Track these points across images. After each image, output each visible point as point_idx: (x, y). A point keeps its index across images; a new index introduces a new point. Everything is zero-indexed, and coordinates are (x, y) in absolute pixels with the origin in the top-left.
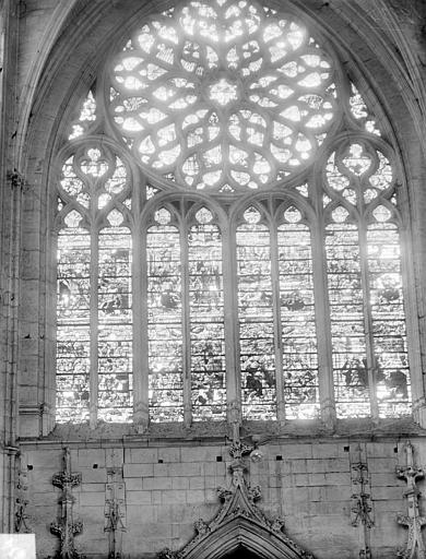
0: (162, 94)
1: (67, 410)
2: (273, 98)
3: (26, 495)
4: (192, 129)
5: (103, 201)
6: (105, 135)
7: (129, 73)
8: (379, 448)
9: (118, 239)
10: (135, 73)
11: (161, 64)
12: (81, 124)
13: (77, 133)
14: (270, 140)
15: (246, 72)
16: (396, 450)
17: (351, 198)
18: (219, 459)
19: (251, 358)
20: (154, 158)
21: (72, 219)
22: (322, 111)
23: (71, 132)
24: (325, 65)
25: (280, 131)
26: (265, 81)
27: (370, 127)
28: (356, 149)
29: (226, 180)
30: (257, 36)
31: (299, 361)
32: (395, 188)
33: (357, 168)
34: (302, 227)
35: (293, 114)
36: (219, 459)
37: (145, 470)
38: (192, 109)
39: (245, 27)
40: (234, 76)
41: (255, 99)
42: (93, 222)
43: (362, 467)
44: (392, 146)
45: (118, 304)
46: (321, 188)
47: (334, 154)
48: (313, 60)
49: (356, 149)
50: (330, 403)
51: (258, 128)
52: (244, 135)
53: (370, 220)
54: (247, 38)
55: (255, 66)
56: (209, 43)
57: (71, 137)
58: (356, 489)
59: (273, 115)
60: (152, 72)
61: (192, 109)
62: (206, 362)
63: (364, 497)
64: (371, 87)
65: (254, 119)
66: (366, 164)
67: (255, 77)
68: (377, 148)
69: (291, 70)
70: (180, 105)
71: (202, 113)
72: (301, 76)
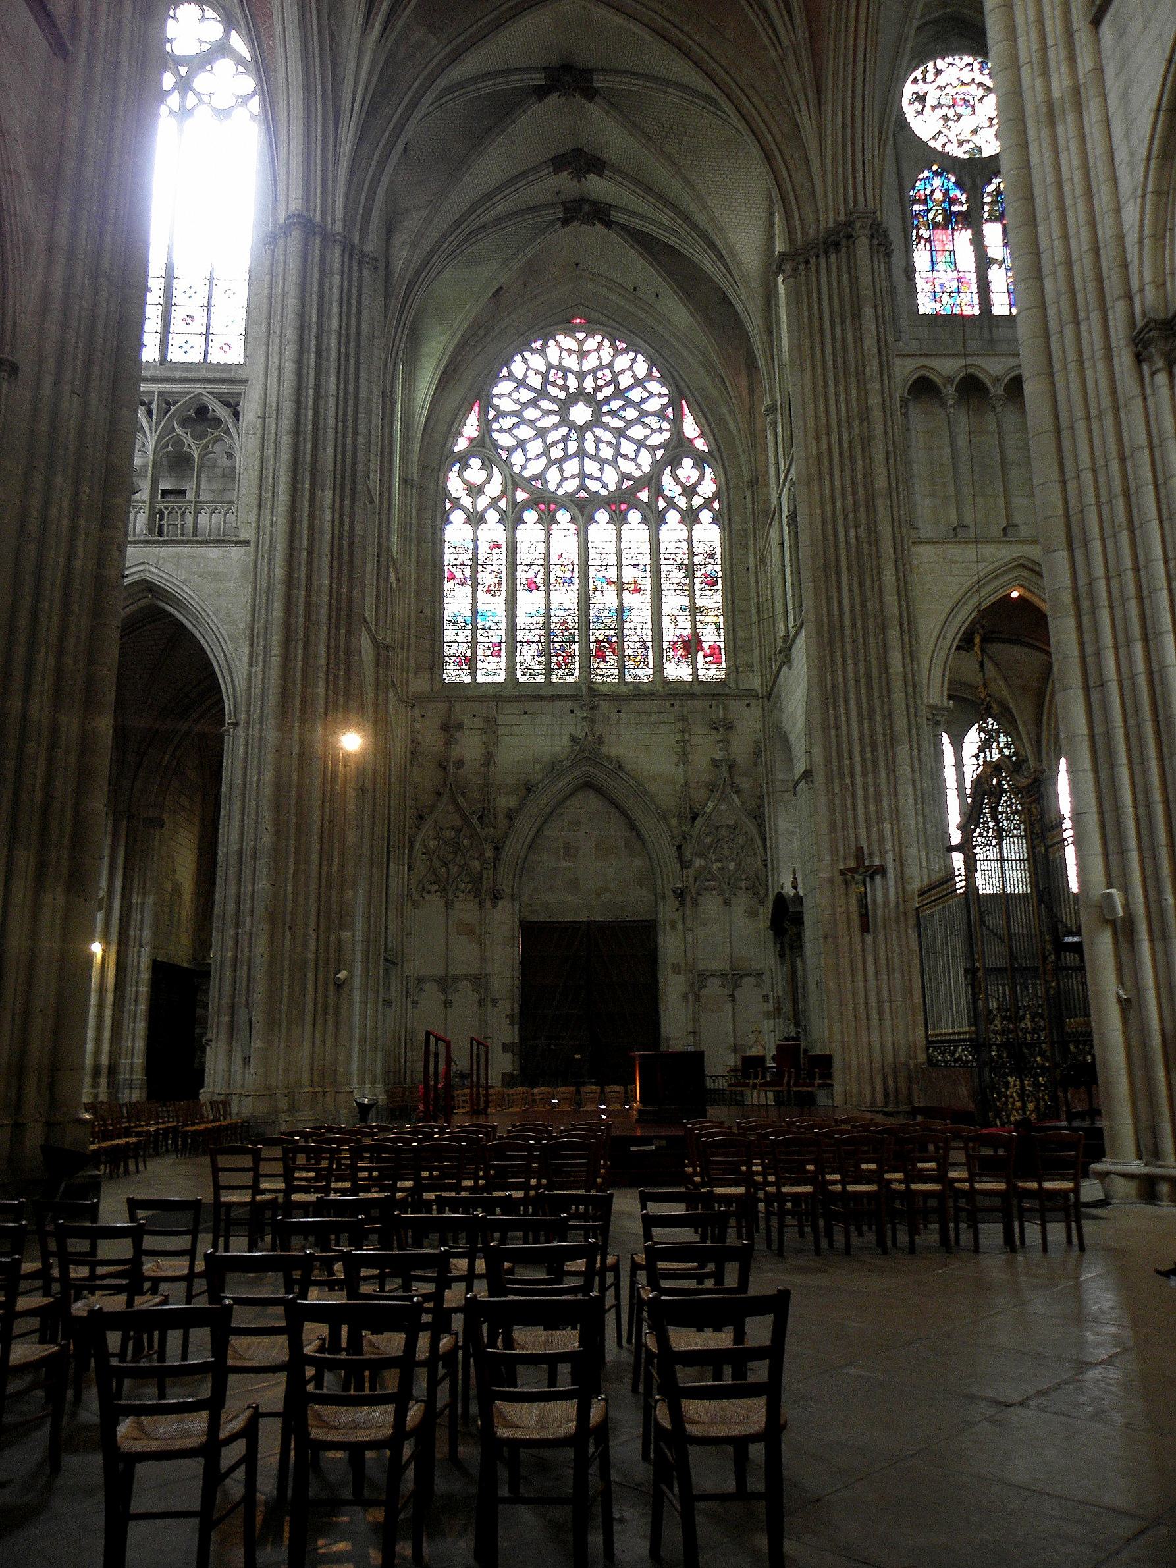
0: (531, 414)
1: (454, 674)
2: (623, 419)
3: (420, 737)
4: (555, 444)
5: (483, 502)
6: (484, 447)
7: (504, 394)
8: (698, 704)
9: (493, 530)
11: (531, 389)
13: (461, 445)
14: (618, 453)
15: (600, 396)
17: (682, 502)
18: (572, 712)
21: (458, 517)
22: (661, 430)
24: (665, 391)
26: (615, 405)
27: (700, 444)
28: (687, 462)
29: (582, 486)
30: (610, 366)
32: (717, 496)
35: (637, 432)
36: (572, 712)
38: (556, 427)
39: (599, 357)
40: (590, 400)
41: (606, 419)
43: (684, 719)
46: (658, 491)
48: (654, 387)
49: (687, 462)
50: (659, 668)
51: (609, 444)
52: (597, 449)
53: (697, 520)
54: (601, 367)
57: (456, 449)
58: (678, 737)
60: (525, 395)
61: (556, 427)
63: (684, 741)
66: (695, 474)
68: (704, 461)
69: (636, 394)
71: (564, 431)
72: (643, 400)
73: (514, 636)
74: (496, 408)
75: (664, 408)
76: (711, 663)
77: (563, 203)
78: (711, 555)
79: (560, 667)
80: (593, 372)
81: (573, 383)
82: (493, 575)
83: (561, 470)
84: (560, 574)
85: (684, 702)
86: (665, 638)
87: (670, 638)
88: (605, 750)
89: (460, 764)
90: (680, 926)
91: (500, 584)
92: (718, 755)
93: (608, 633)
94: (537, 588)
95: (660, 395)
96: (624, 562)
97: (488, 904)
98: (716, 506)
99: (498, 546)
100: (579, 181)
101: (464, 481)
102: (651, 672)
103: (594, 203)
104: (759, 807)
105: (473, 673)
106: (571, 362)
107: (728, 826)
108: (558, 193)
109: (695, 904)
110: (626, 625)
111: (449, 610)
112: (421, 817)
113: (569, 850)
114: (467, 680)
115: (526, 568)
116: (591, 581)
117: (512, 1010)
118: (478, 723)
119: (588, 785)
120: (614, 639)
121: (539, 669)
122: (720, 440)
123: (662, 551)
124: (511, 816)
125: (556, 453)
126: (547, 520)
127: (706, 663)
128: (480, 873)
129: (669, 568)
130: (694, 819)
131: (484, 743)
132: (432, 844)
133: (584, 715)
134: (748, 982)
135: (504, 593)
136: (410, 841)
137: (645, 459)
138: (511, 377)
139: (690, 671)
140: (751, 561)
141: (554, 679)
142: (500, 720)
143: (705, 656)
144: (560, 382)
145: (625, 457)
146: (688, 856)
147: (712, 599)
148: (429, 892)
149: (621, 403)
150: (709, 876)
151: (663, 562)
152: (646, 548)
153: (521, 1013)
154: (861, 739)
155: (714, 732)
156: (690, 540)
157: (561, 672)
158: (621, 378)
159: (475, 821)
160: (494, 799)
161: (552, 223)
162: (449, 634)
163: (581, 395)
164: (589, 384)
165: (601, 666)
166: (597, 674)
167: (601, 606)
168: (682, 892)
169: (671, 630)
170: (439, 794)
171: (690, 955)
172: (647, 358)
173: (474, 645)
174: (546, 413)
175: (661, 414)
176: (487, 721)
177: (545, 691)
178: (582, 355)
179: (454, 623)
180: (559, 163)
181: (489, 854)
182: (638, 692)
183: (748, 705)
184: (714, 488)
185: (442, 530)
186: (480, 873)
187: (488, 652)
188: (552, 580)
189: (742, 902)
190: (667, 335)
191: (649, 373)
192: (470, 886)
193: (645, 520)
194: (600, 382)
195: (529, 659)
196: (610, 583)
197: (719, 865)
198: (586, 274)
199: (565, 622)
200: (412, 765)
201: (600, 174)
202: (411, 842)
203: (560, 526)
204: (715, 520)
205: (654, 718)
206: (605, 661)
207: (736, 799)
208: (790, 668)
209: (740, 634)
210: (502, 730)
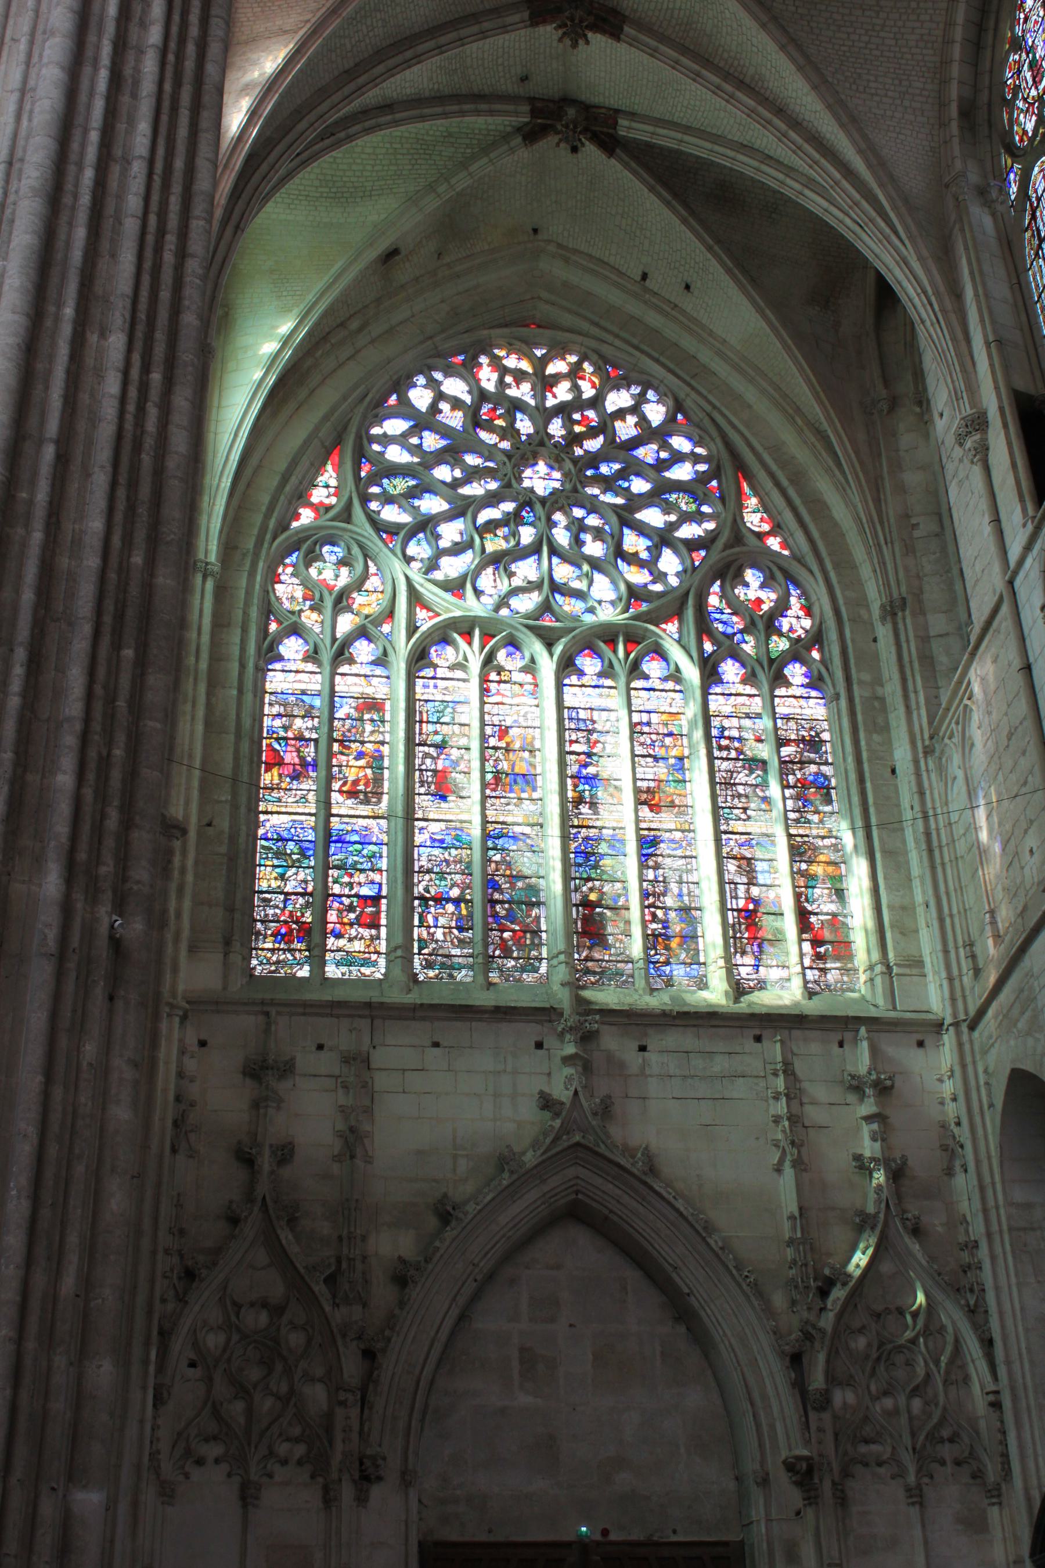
0: (443, 473)
4: (491, 526)
5: (345, 624)
10: (401, 440)
11: (444, 431)
12: (315, 507)
13: (306, 516)
17: (749, 647)
19: (590, 884)
21: (292, 648)
22: (698, 517)
23: (297, 516)
25: (633, 542)
30: (596, 402)
32: (817, 638)
33: (759, 601)
35: (653, 517)
39: (576, 388)
42: (326, 656)
44: (811, 572)
45: (366, 785)
47: (718, 583)
48: (681, 443)
49: (752, 576)
51: (598, 534)
52: (578, 543)
53: (779, 679)
54: (578, 404)
55: (594, 445)
56: (517, 406)
59: (625, 517)
60: (431, 441)
61: (492, 499)
62: (513, 886)
64: (777, 484)
65: (593, 521)
66: (769, 598)
67: (594, 460)
70: (474, 489)
71: (509, 507)
72: (661, 466)
73: (409, 885)
75: (701, 479)
77: (531, 100)
78: (813, 744)
79: (507, 954)
80: (563, 410)
81: (525, 426)
82: (362, 763)
87: (741, 903)
89: (285, 1153)
95: (696, 459)
97: (347, 1492)
98: (815, 655)
101: (306, 583)
103: (587, 109)
105: (318, 961)
106: (523, 392)
108: (524, 79)
109: (842, 1500)
111: (272, 823)
112: (190, 1275)
114: (304, 972)
115: (432, 751)
116: (569, 781)
118: (327, 1063)
122: (816, 534)
123: (715, 732)
125: (495, 544)
128: (330, 1415)
130: (824, 1293)
131: (342, 1109)
132: (213, 1341)
133: (570, 1049)
136: (161, 1333)
137: (670, 563)
138: (406, 410)
142: (379, 1058)
144: (500, 422)
145: (632, 559)
146: (817, 1380)
148: (200, 1462)
149: (617, 466)
151: (716, 753)
155: (851, 1098)
158: (618, 424)
159: (320, 1288)
160: (364, 1238)
161: (506, 137)
162: (266, 878)
163: (542, 444)
166: (588, 971)
168: (810, 1471)
169: (741, 890)
170: (234, 1221)
173: (321, 898)
174: (473, 475)
177: (484, 999)
178: (545, 383)
179: (278, 855)
181: (352, 1367)
184: (807, 623)
185: (262, 672)
186: (330, 1415)
187: (352, 916)
190: (705, 356)
192: (300, 1450)
194: (578, 429)
195: (439, 934)
197: (888, 1403)
198: (552, 248)
200: (174, 1150)
201: (616, 34)
202: (165, 1335)
204: (815, 682)
207: (915, 1247)
210: (381, 1081)
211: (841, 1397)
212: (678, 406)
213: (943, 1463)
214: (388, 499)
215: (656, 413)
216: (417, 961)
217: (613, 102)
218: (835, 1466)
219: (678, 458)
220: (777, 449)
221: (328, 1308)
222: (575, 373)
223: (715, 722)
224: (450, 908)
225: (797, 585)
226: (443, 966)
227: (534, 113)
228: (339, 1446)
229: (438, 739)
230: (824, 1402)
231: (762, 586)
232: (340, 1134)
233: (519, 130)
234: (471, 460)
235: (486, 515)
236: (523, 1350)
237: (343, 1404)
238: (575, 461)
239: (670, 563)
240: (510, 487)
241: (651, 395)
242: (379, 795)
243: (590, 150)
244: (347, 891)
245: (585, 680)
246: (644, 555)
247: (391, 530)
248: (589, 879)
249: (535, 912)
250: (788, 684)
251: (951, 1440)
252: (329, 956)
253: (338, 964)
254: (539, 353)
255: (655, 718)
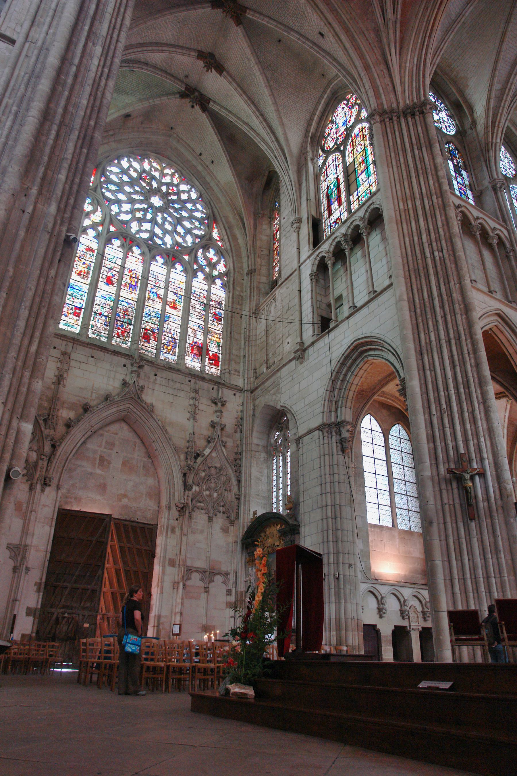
4: (139, 210)
8: (206, 385)
10: (117, 174)
11: (130, 177)
16: (213, 389)
20: (118, 214)
22: (200, 229)
25: (179, 229)
29: (151, 238)
30: (177, 186)
31: (170, 333)
32: (227, 274)
33: (212, 259)
34: (182, 274)
35: (187, 224)
36: (125, 366)
37: (83, 359)
40: (164, 196)
43: (196, 392)
48: (199, 206)
50: (181, 357)
51: (170, 223)
52: (163, 224)
53: (214, 282)
55: (174, 198)
56: (153, 178)
58: (192, 402)
59: (179, 221)
61: (141, 202)
62: (124, 317)
64: (224, 227)
65: (169, 219)
66: (215, 259)
67: (173, 202)
69: (189, 206)
71: (146, 206)
73: (92, 308)
74: (107, 177)
75: (203, 219)
76: (212, 364)
77: (187, 85)
78: (220, 303)
79: (119, 336)
80: (167, 184)
82: (85, 266)
83: (141, 225)
84: (129, 281)
85: (198, 382)
86: (188, 341)
87: (191, 342)
88: (144, 397)
90: (178, 531)
91: (88, 273)
92: (216, 419)
93: (153, 326)
94: (112, 283)
95: (203, 213)
96: (170, 289)
97: (39, 487)
99: (93, 251)
100: (207, 71)
102: (176, 358)
103: (201, 95)
104: (236, 460)
106: (157, 174)
107: (216, 467)
109: (190, 517)
110: (166, 326)
113: (103, 462)
115: (107, 270)
116: (147, 292)
117: (41, 579)
118: (56, 353)
119: (124, 420)
120: (156, 331)
121: (104, 333)
122: (232, 245)
124: (69, 425)
125: (139, 215)
126: (127, 248)
127: (209, 363)
129: (195, 302)
130: (196, 458)
131: (58, 369)
134: (219, 579)
135: (89, 279)
137: (189, 239)
138: (119, 166)
139: (199, 365)
140: (246, 312)
141: (113, 342)
142: (73, 356)
143: (210, 359)
145: (179, 234)
146: (190, 481)
147: (217, 328)
149: (179, 206)
150: (201, 499)
152: (183, 286)
153: (46, 584)
154: (455, 378)
155: (213, 405)
156: (209, 291)
157: (119, 340)
158: (182, 194)
159: (41, 422)
160: (58, 410)
164: (164, 189)
165: (146, 344)
167: (152, 309)
169: (191, 338)
171: (183, 552)
172: (197, 191)
174: (136, 193)
175: (201, 221)
176: (64, 354)
180: (201, 55)
181: (47, 449)
182: (168, 367)
183: (234, 394)
184: (224, 269)
187: (72, 311)
188: (123, 283)
189: (220, 521)
190: (212, 184)
191: (198, 199)
193: (185, 270)
194: (170, 191)
195: (98, 325)
196: (158, 296)
197: (208, 493)
199: (126, 310)
203: (134, 255)
204: (224, 286)
205: (178, 385)
206: (149, 343)
208: (301, 363)
209: (234, 352)
210: (73, 363)
211: (195, 488)
212: (201, 196)
213: (220, 512)
214: (108, 190)
215: (194, 195)
216: (90, 330)
217: (210, 96)
218: (190, 508)
219: (197, 210)
220: (226, 218)
221: (43, 429)
222: (172, 175)
223: (193, 288)
224: (104, 318)
225: (224, 258)
226: (98, 335)
227: (186, 89)
228: (38, 473)
229: (110, 267)
230: (190, 489)
231: (214, 255)
232: (55, 376)
233: (179, 93)
234: (137, 188)
235: (137, 206)
236: (101, 456)
237: (41, 459)
238: (168, 200)
239: (189, 239)
240: (147, 200)
241: (193, 189)
242: (87, 277)
243: (198, 108)
244: (71, 303)
245: (157, 264)
246: (182, 234)
247: (108, 200)
248: (147, 322)
249: (129, 327)
250: (216, 285)
251: (223, 506)
252: (61, 321)
253: (64, 325)
254: (164, 165)
255: (176, 282)
